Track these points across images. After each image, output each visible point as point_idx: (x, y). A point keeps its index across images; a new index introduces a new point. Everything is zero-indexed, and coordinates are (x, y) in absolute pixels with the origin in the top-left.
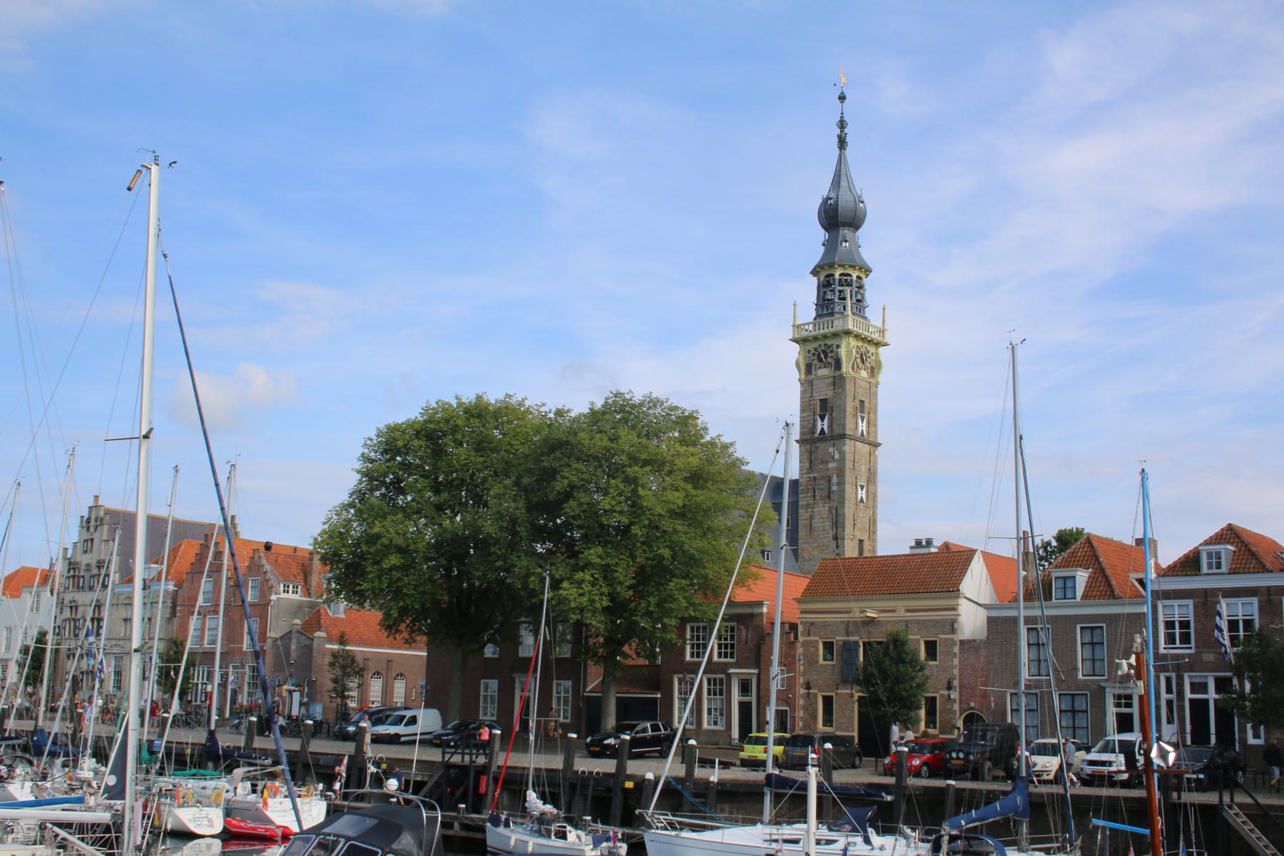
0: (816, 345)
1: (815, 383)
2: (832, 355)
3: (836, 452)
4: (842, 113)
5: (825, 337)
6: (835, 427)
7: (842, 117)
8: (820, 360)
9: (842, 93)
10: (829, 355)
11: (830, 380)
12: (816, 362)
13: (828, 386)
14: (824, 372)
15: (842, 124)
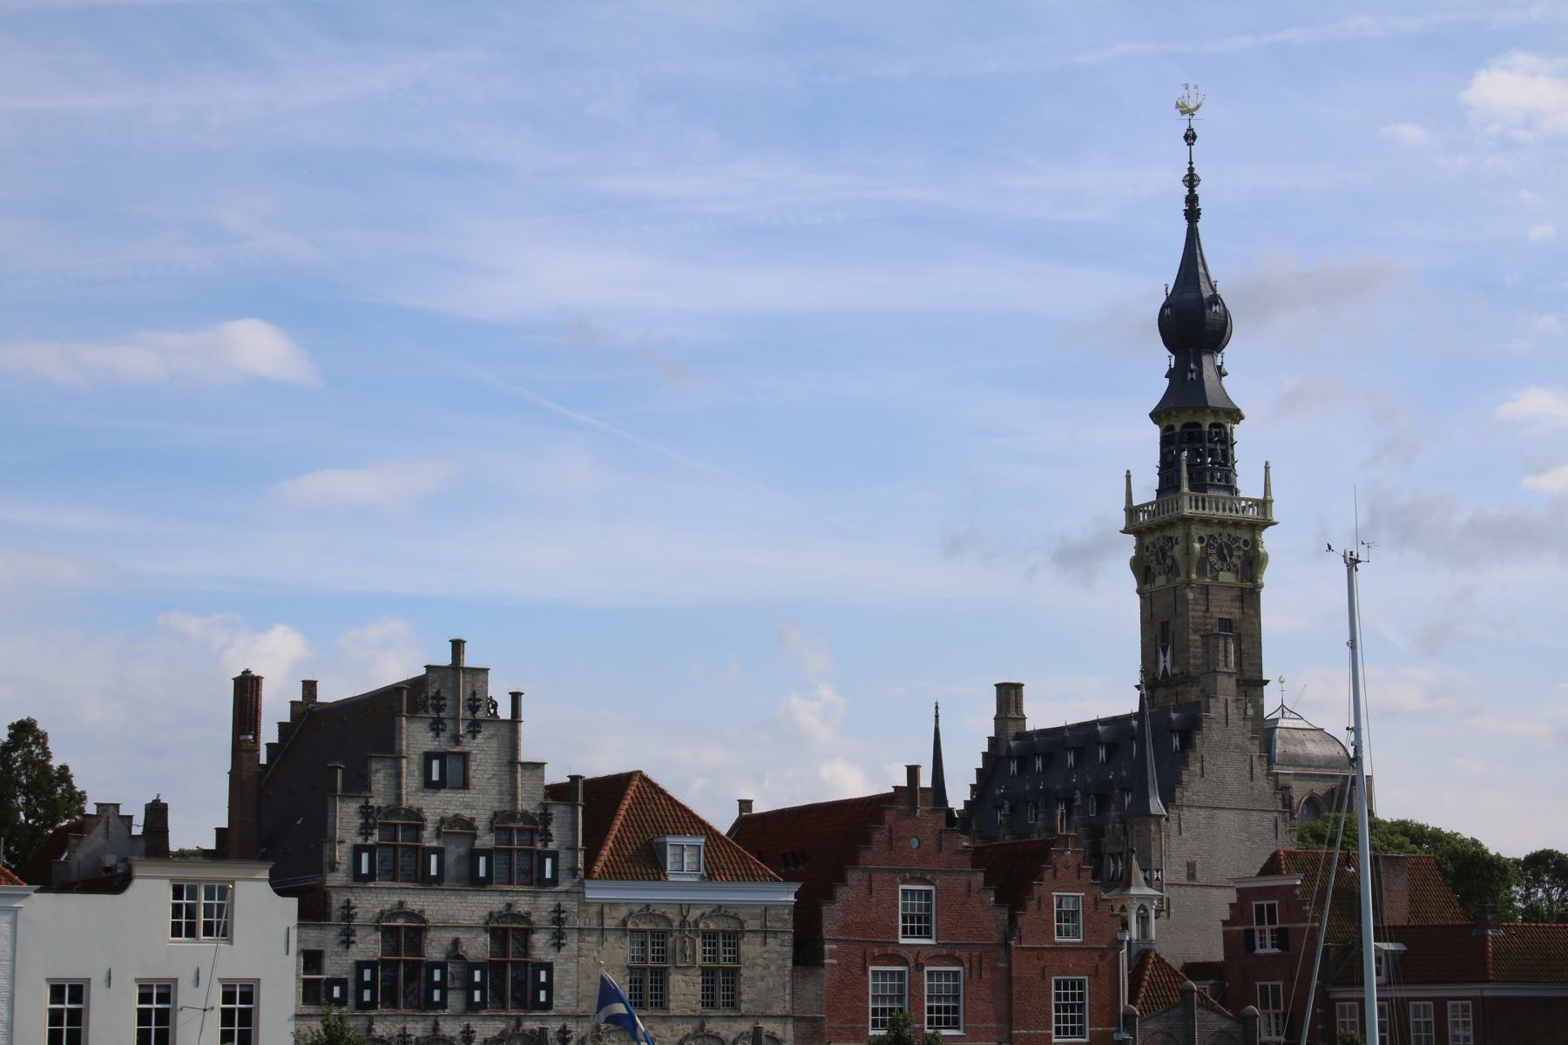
0: (1216, 531)
1: (1211, 590)
2: (1240, 553)
3: (1249, 705)
4: (1191, 163)
5: (1237, 524)
6: (1245, 666)
7: (1191, 169)
8: (1222, 558)
9: (1190, 129)
10: (1235, 553)
11: (1236, 593)
12: (1214, 558)
13: (1232, 601)
14: (1226, 577)
15: (1191, 180)
